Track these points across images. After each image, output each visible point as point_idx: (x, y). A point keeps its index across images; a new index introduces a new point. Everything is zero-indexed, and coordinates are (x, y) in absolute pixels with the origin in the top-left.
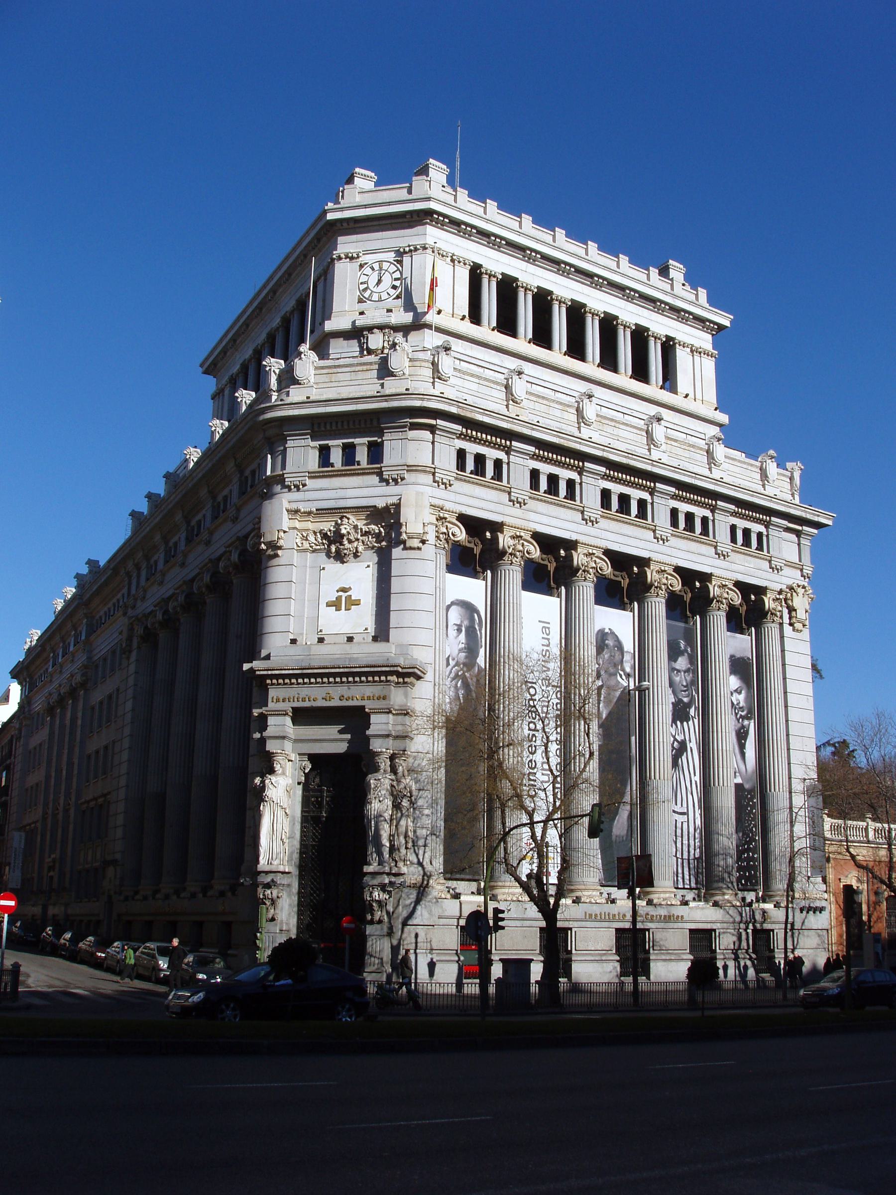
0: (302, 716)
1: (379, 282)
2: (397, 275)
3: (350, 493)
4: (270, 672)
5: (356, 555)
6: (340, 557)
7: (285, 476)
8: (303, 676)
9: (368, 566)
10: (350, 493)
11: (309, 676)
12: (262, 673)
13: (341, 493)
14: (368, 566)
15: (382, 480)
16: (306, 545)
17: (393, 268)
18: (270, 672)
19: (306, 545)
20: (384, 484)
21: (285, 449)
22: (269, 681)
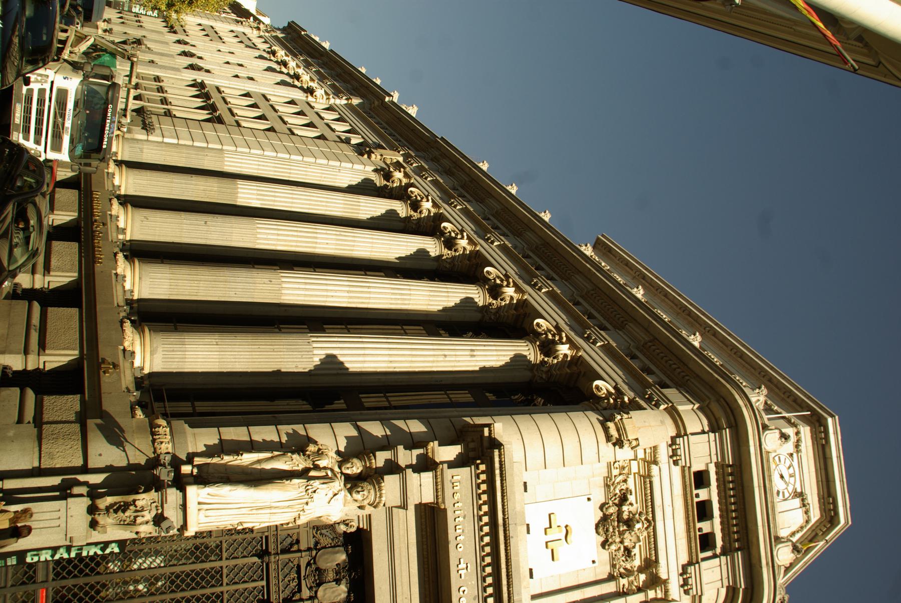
0: (431, 521)
1: (782, 477)
2: (787, 495)
3: (669, 522)
4: (497, 472)
5: (604, 544)
6: (603, 523)
7: (685, 437)
8: (493, 523)
9: (594, 562)
10: (669, 522)
11: (494, 534)
12: (497, 459)
13: (668, 510)
14: (594, 562)
15: (684, 567)
16: (615, 472)
17: (791, 488)
18: (497, 472)
19: (615, 472)
20: (681, 571)
21: (707, 433)
22: (483, 467)
